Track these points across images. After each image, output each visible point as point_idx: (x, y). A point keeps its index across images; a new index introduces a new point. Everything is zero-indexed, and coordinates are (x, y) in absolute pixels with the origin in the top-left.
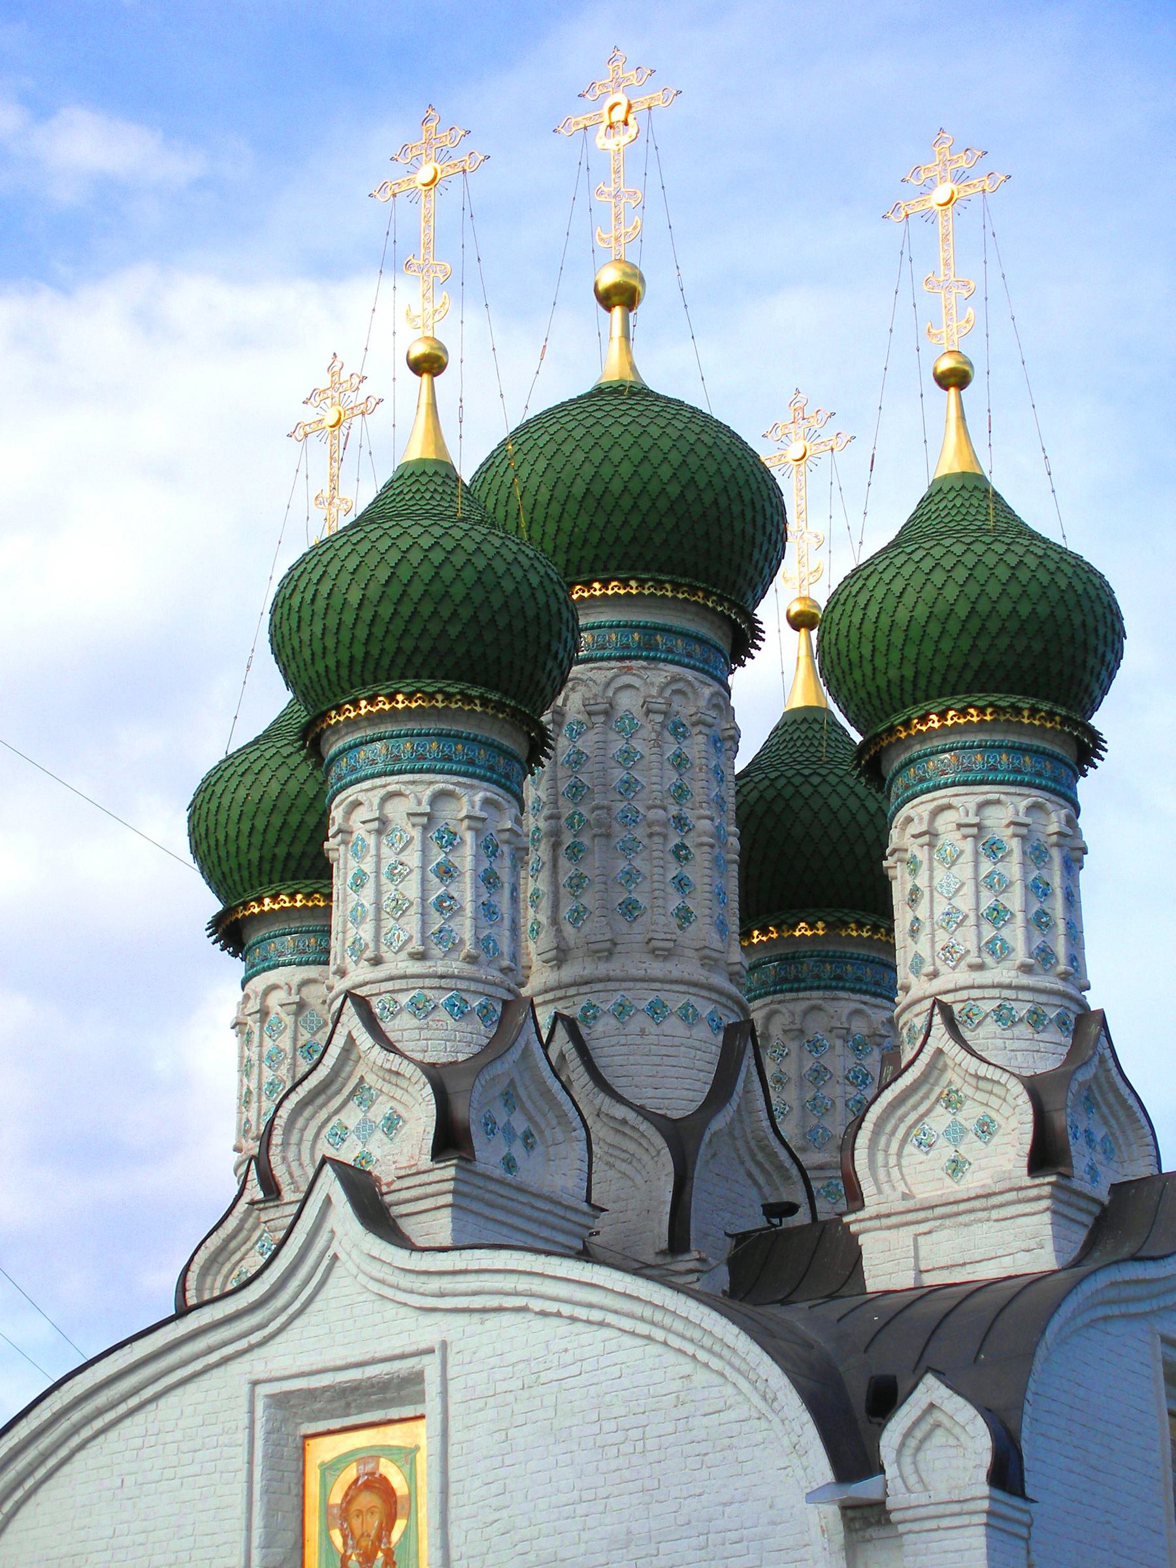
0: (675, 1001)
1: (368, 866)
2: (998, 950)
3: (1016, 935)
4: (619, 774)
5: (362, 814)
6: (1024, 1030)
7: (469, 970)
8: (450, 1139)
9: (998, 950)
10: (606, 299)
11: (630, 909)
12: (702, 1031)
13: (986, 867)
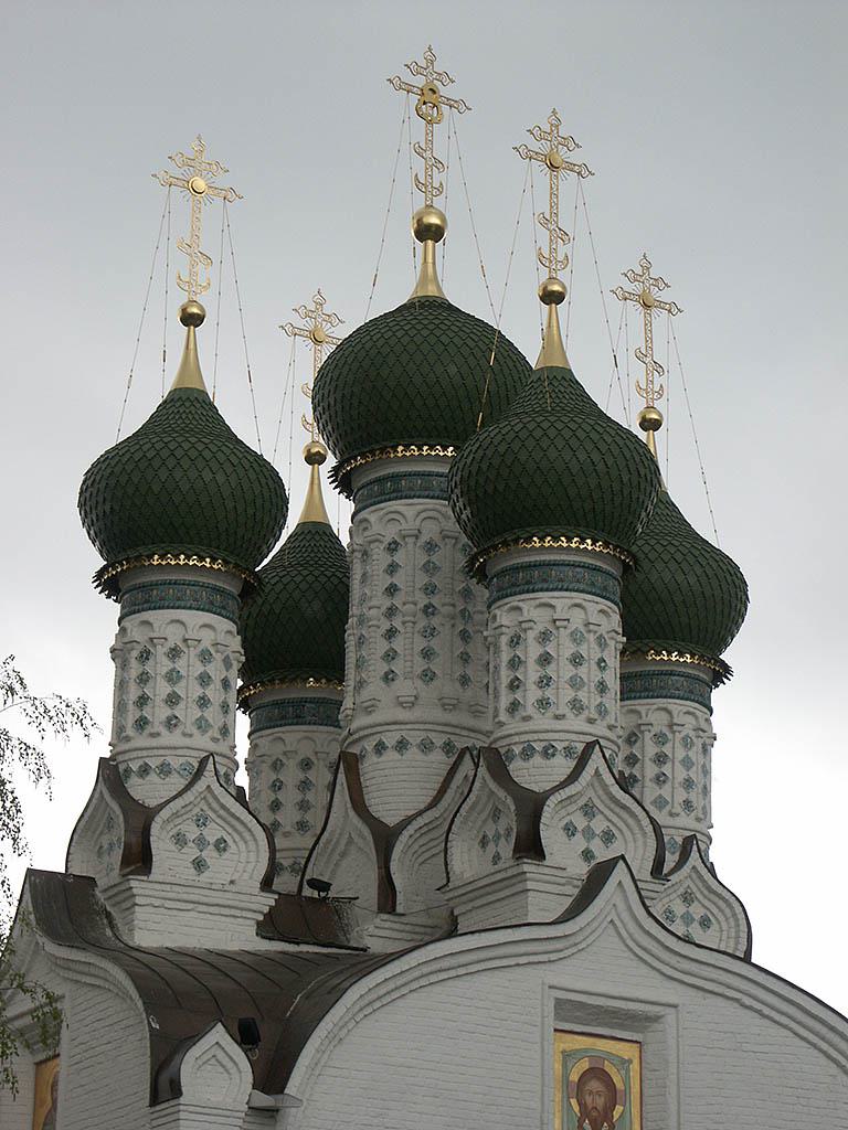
0: (415, 738)
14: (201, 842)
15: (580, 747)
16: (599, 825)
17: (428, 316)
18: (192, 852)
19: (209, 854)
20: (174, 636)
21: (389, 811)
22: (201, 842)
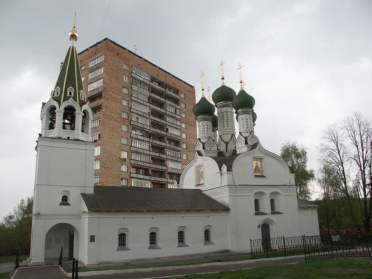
0: (227, 133)
1: (202, 128)
2: (244, 127)
3: (245, 126)
4: (223, 116)
5: (201, 124)
6: (246, 133)
7: (206, 135)
8: (204, 148)
9: (244, 127)
10: (222, 79)
11: (224, 127)
13: (243, 121)
14: (210, 146)
17: (223, 87)
21: (227, 140)
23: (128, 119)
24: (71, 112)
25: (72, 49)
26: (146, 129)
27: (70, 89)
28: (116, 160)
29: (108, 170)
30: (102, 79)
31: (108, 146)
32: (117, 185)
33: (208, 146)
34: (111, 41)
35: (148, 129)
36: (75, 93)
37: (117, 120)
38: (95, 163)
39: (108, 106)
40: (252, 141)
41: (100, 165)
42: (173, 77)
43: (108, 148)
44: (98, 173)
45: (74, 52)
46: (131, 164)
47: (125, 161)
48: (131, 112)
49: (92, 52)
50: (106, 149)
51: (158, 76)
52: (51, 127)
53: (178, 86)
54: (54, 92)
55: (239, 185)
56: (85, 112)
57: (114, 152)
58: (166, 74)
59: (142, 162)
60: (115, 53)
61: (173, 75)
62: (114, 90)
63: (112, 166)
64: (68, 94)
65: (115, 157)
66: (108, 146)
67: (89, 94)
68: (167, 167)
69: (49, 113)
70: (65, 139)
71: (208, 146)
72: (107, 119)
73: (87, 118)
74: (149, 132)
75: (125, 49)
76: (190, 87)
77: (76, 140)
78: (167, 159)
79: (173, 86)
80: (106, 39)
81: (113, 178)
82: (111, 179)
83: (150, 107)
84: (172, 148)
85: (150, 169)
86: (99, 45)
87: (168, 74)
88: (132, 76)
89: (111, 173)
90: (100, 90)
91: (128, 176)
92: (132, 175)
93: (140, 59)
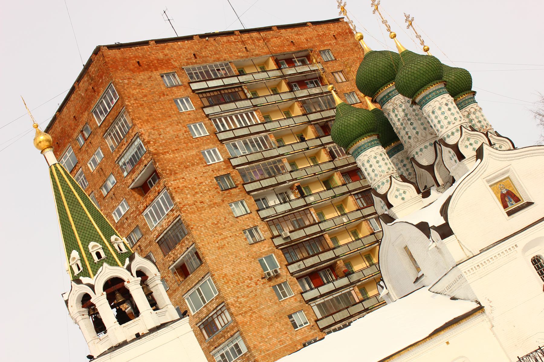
11: (409, 138)
12: (429, 147)
14: (400, 194)
15: (459, 128)
16: (472, 141)
18: (400, 197)
19: (403, 195)
20: (366, 158)
22: (400, 194)
23: (236, 187)
24: (119, 286)
25: (56, 170)
26: (285, 182)
27: (92, 248)
28: (256, 284)
29: (251, 316)
30: (138, 140)
31: (226, 267)
32: (286, 333)
33: (396, 197)
34: (110, 47)
35: (289, 181)
36: (105, 248)
37: (216, 203)
38: (220, 314)
39: (181, 186)
40: (471, 144)
41: (231, 314)
42: (283, 31)
43: (227, 270)
44: (235, 331)
45: (61, 174)
46: (292, 274)
47: (277, 275)
48: (234, 167)
49: (86, 91)
50: (226, 275)
51: (247, 51)
52: (100, 326)
53: (302, 38)
54: (71, 267)
55: (482, 251)
56: (140, 273)
57: (244, 271)
58: (263, 34)
59: (313, 256)
60: (132, 67)
61: (280, 27)
62: (174, 146)
63: (257, 302)
64: (96, 259)
65: (251, 279)
66: (226, 267)
67: (130, 181)
68: (373, 234)
69: (84, 309)
70: (133, 340)
71: (396, 197)
72: (193, 213)
73: (149, 279)
74: (294, 184)
75: (146, 43)
76: (331, 25)
77: (152, 331)
78: (364, 217)
79: (293, 49)
80: (98, 50)
81: (271, 325)
82: (266, 330)
83: (269, 131)
84: (363, 187)
85: (338, 262)
86: (92, 69)
87: (268, 33)
88: (194, 91)
89: (261, 317)
90: (146, 162)
91: (300, 301)
92: (308, 296)
93: (190, 42)
